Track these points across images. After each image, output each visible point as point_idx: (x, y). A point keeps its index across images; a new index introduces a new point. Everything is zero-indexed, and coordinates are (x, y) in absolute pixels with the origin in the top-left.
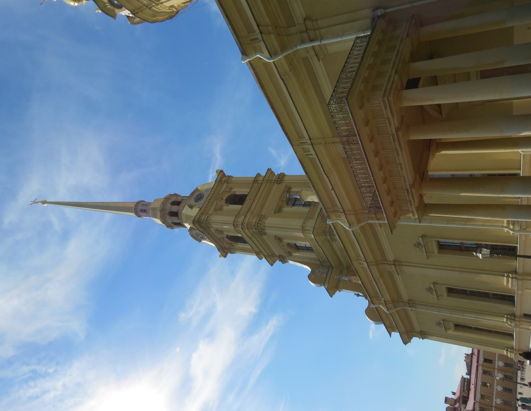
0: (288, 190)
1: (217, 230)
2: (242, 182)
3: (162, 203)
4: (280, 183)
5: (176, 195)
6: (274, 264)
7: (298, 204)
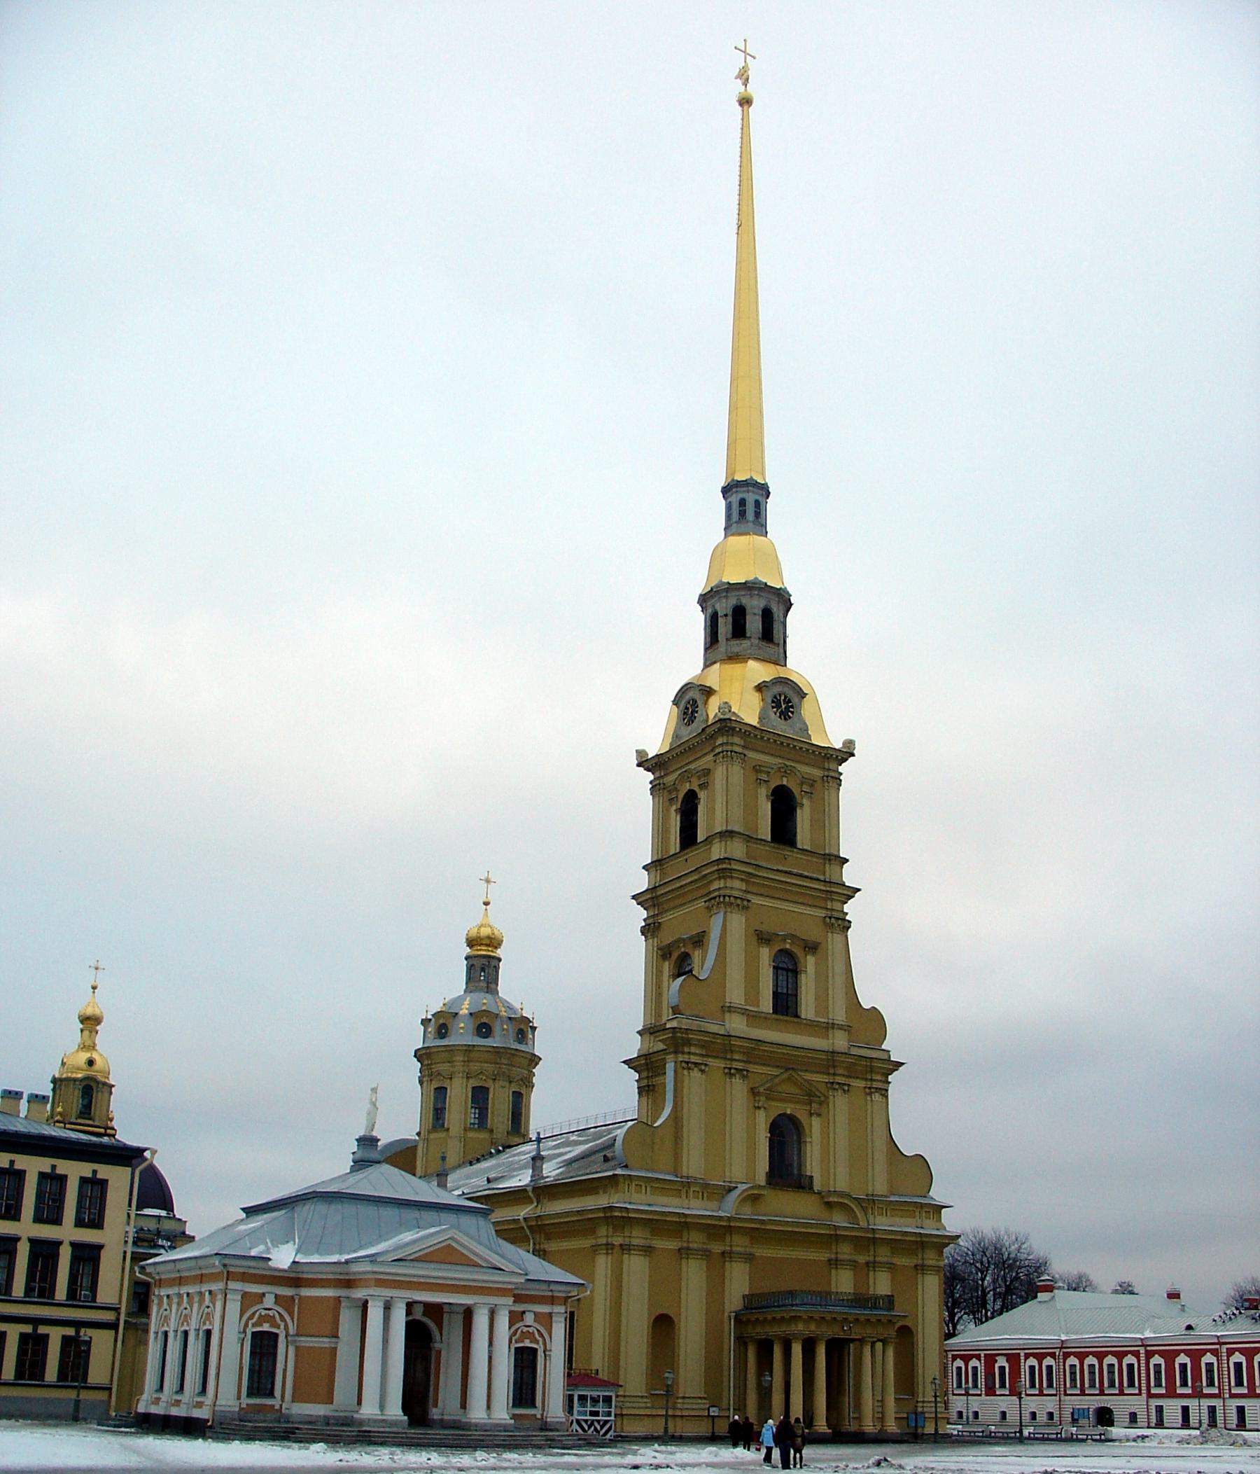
0: (812, 948)
1: (707, 772)
2: (828, 819)
3: (766, 584)
5: (788, 605)
6: (634, 902)
7: (780, 978)
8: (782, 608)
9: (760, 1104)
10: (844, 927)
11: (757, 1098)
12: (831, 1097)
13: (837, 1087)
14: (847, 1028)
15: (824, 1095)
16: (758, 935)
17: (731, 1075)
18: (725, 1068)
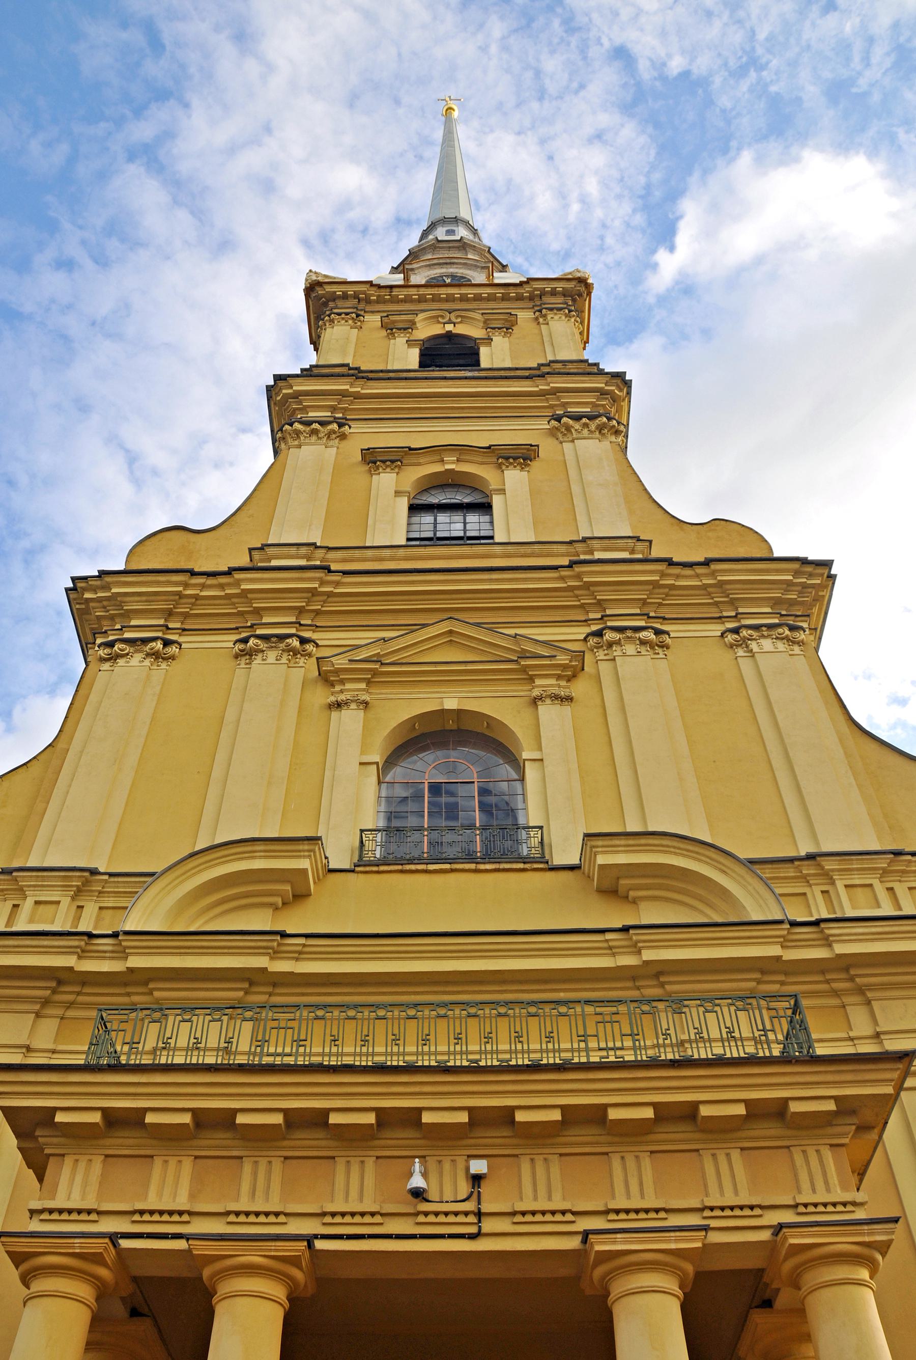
17: (250, 654)
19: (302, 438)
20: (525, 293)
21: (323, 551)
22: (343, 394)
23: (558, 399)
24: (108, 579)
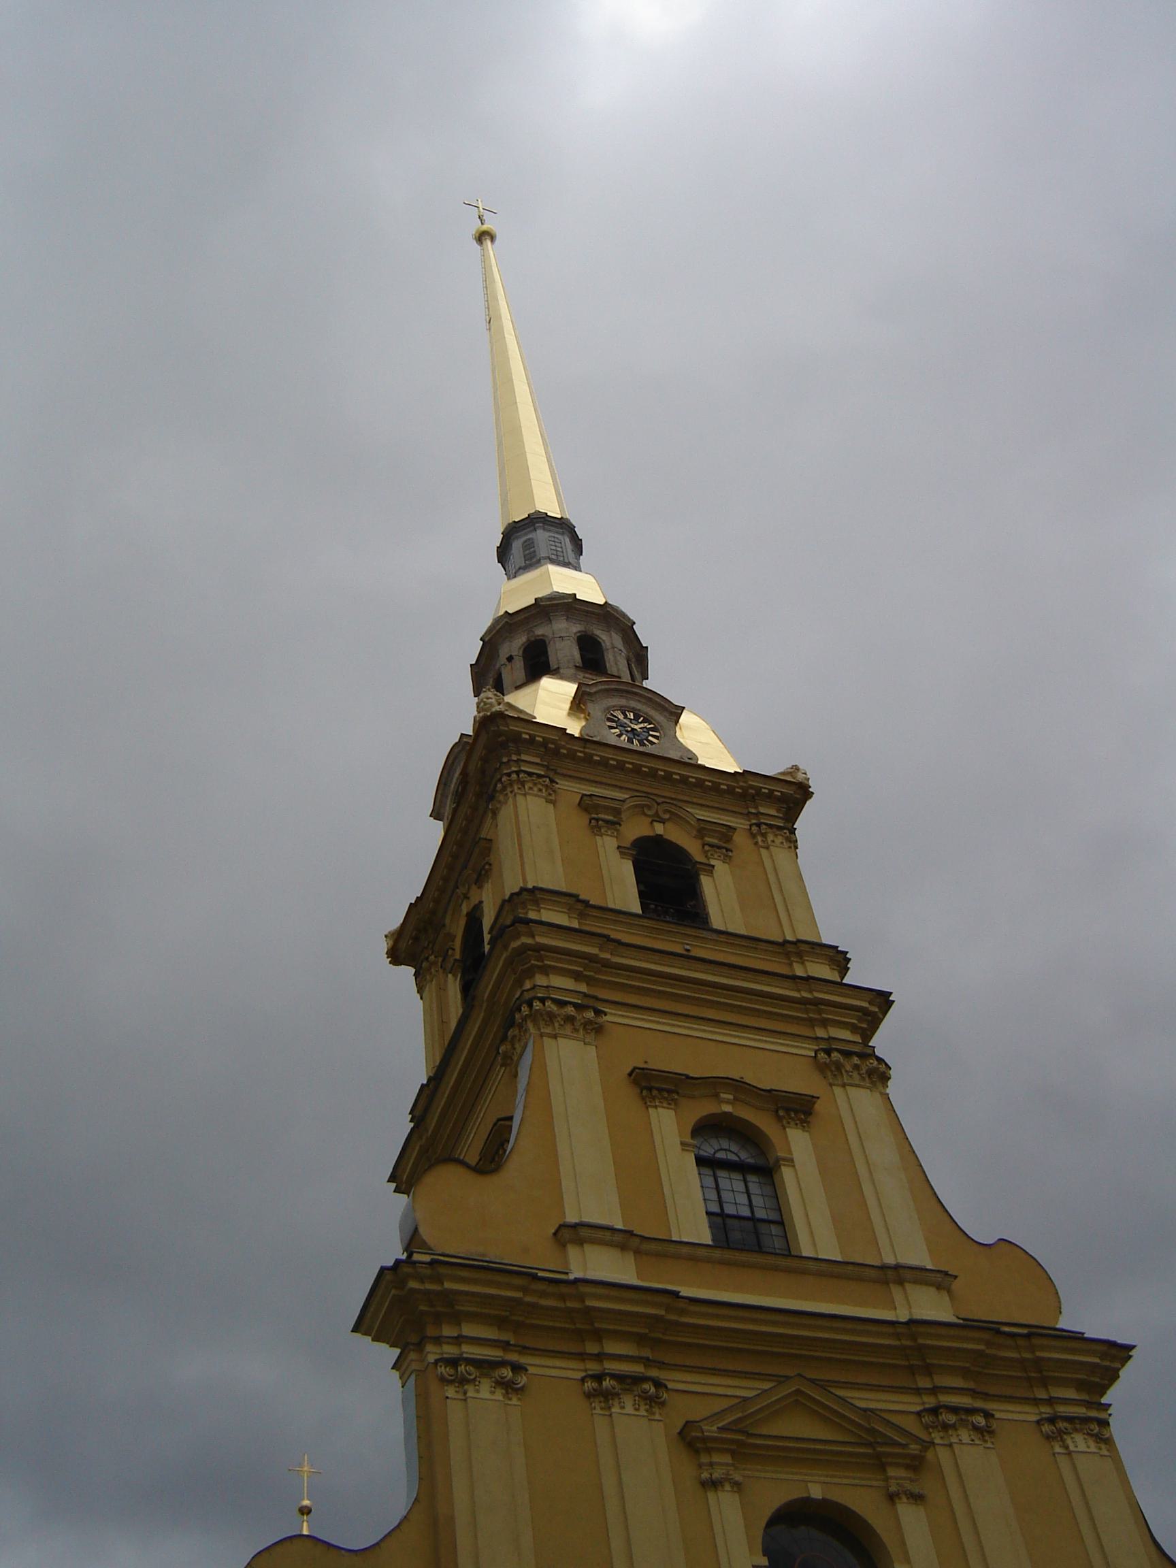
4: (822, 1068)
8: (618, 641)
9: (717, 1474)
10: (871, 1072)
11: (705, 1459)
12: (943, 1455)
13: (951, 1419)
14: (941, 1280)
15: (917, 1439)
16: (636, 1082)
17: (607, 1397)
18: (583, 1380)
19: (556, 1025)
20: (738, 788)
21: (637, 1240)
22: (591, 958)
23: (820, 1012)
24: (442, 1270)
